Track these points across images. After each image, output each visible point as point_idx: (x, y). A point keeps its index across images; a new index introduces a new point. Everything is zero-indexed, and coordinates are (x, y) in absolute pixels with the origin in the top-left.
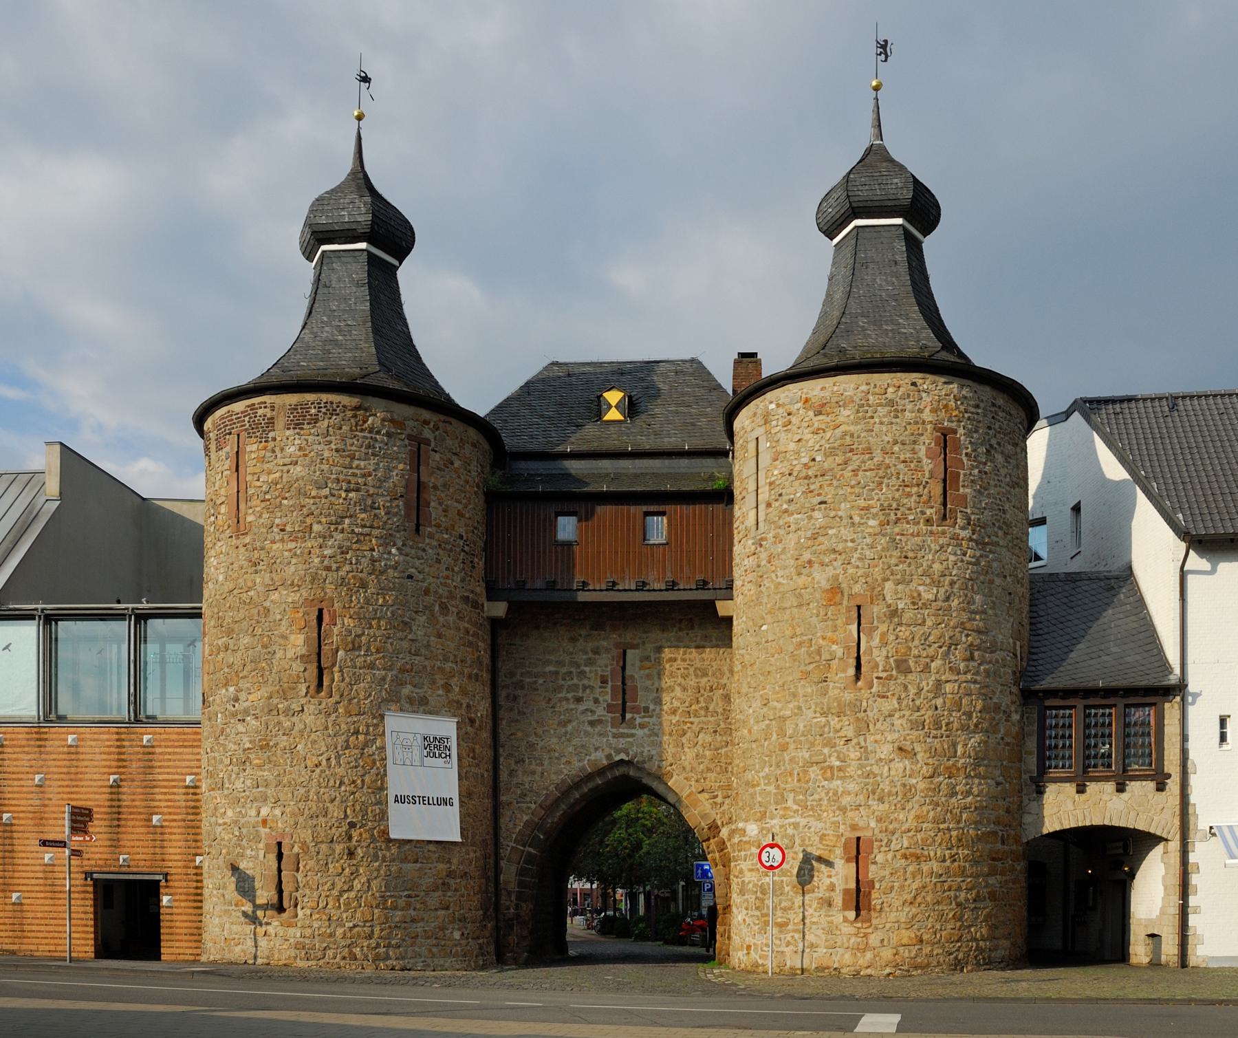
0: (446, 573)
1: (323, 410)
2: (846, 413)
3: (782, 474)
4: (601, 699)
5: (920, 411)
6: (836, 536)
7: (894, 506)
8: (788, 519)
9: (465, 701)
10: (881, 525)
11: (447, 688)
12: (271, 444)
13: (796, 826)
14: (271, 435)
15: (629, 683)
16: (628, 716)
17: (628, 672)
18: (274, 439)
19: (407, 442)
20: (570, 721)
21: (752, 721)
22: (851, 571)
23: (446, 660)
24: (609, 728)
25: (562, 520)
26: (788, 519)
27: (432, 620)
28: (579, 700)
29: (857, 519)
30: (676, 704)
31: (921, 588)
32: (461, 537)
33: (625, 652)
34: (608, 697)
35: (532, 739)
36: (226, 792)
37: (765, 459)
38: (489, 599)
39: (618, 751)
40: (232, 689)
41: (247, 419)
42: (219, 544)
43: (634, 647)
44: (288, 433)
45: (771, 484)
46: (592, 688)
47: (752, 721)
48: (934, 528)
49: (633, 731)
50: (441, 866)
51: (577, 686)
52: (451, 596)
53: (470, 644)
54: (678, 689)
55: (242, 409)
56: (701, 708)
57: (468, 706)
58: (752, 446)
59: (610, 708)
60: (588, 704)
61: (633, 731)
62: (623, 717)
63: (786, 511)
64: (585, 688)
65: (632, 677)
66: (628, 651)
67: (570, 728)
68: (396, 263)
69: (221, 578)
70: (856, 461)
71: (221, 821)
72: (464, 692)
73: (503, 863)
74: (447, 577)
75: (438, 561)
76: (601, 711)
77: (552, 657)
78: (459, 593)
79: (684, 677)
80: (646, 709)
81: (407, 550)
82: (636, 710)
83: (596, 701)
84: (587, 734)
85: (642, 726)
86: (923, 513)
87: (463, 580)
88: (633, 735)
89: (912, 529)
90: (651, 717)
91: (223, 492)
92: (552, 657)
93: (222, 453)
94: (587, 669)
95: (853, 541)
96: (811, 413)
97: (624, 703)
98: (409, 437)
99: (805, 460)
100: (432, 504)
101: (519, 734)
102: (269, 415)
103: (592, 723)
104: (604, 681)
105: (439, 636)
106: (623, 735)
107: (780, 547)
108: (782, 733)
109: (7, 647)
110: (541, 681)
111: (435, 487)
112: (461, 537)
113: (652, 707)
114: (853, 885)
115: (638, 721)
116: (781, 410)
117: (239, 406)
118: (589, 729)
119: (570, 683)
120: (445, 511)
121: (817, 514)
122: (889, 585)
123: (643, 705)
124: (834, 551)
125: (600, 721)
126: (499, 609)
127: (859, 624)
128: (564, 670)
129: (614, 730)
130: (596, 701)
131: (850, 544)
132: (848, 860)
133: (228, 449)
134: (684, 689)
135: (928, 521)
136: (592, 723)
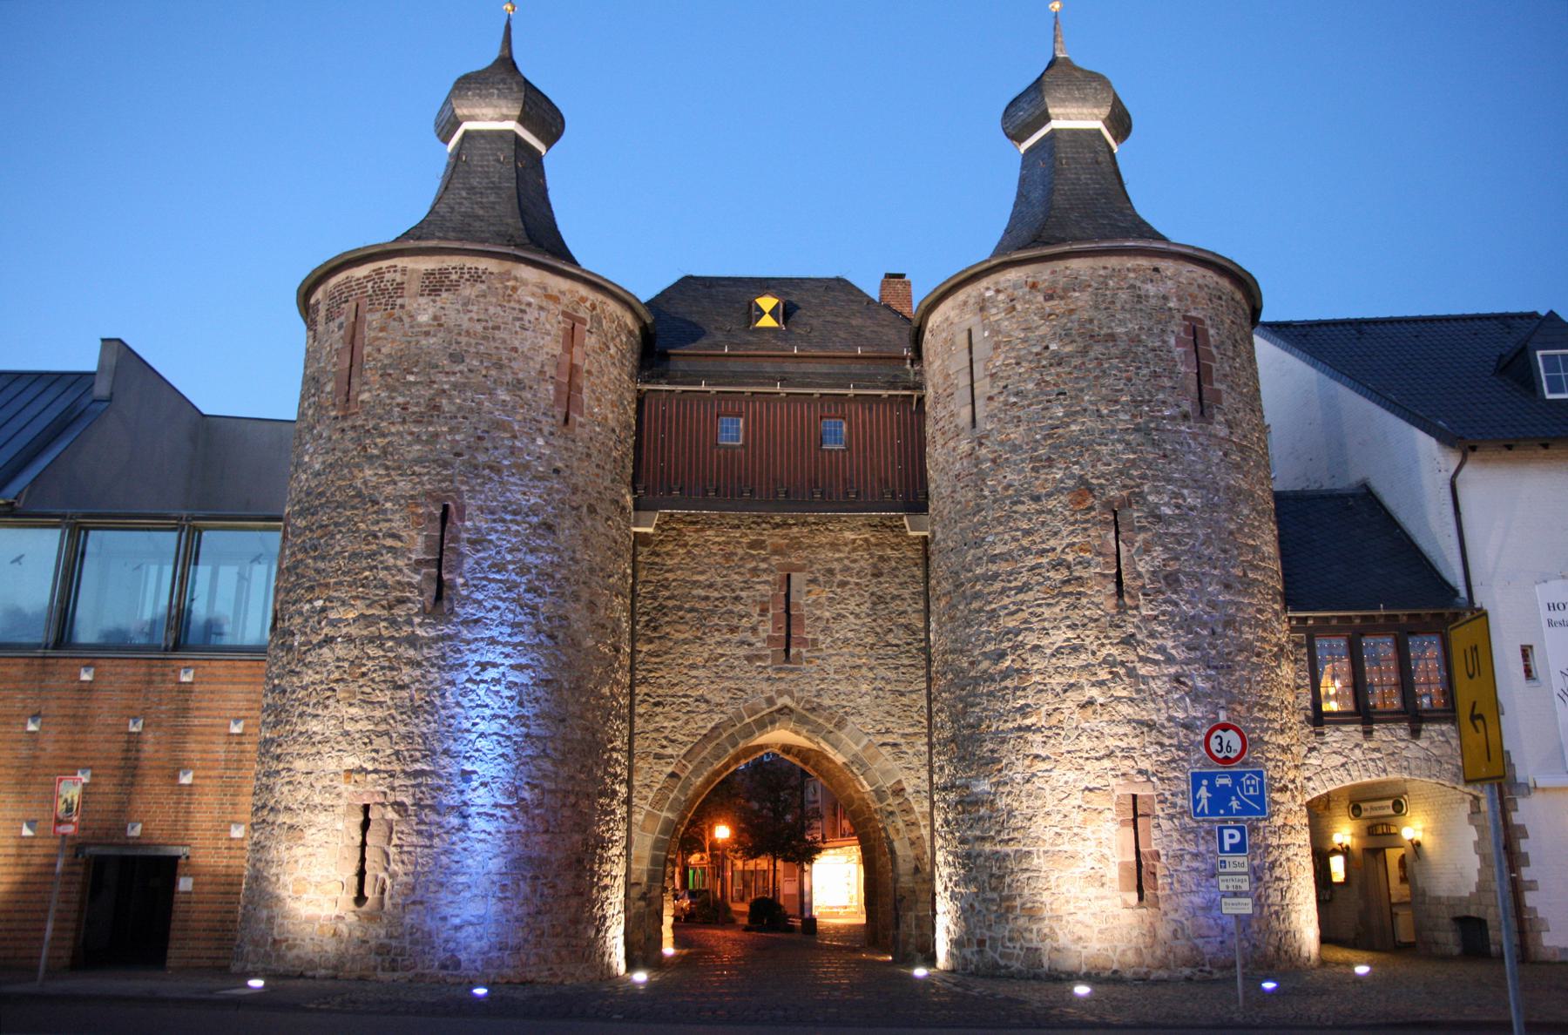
2: (1081, 298)
5: (1165, 298)
12: (397, 312)
14: (399, 301)
16: (793, 651)
18: (402, 306)
19: (560, 318)
25: (725, 422)
34: (769, 626)
43: (800, 569)
45: (992, 375)
58: (962, 339)
62: (787, 651)
65: (798, 604)
66: (794, 575)
68: (541, 147)
70: (1097, 350)
80: (815, 641)
93: (333, 325)
96: (1040, 298)
97: (788, 635)
98: (564, 313)
109: (18, 560)
114: (1133, 858)
116: (1001, 297)
127: (1117, 533)
132: (1123, 823)
135: (1185, 417)
136: (749, 659)
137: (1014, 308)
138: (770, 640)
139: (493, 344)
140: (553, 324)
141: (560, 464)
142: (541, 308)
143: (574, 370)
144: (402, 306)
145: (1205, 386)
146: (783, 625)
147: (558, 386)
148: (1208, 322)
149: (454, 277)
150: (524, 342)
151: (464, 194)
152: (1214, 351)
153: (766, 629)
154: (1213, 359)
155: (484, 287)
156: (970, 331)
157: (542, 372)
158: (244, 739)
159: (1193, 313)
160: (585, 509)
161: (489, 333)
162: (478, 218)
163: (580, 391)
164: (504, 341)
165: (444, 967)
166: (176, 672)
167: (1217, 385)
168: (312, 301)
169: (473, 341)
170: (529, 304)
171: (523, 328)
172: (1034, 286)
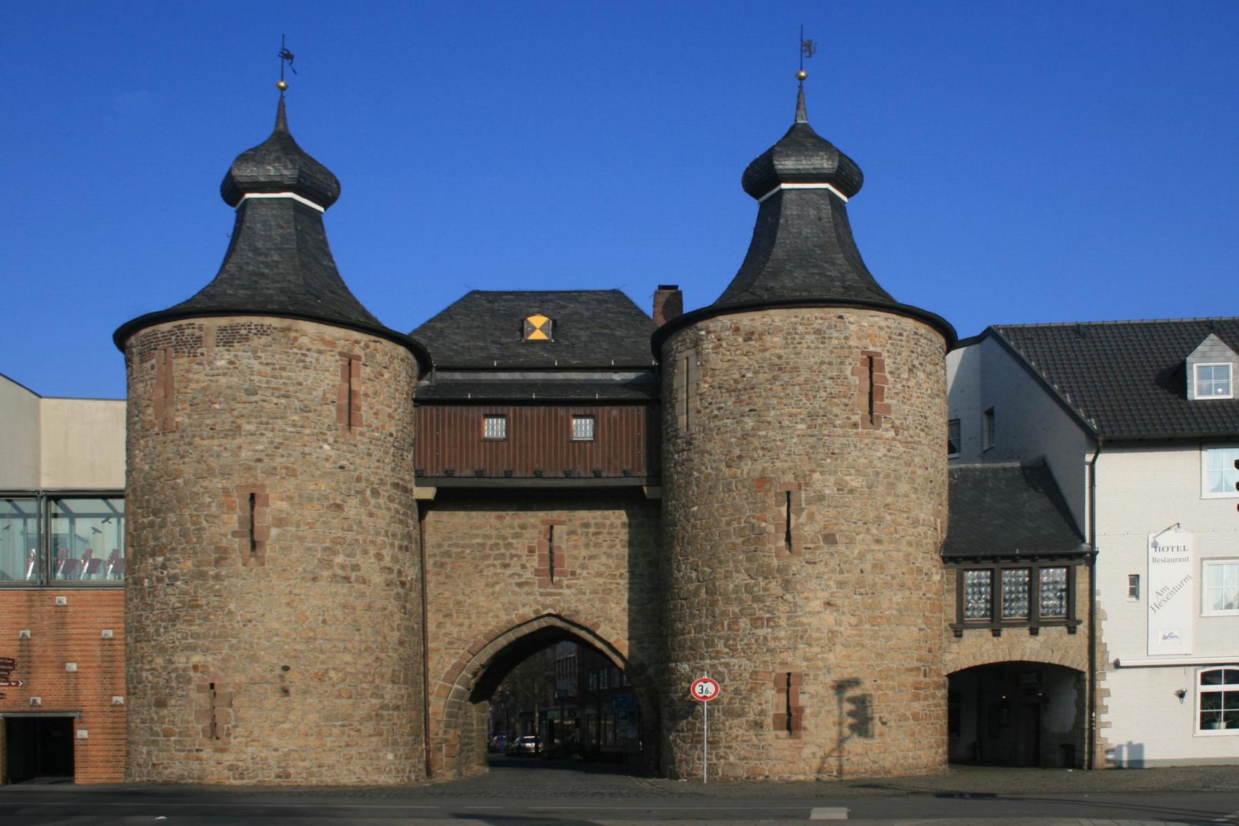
0: (377, 464)
8: (718, 423)
9: (396, 568)
11: (379, 557)
14: (199, 351)
16: (556, 579)
17: (556, 542)
20: (497, 583)
23: (378, 534)
26: (718, 423)
27: (364, 502)
32: (391, 435)
35: (460, 597)
38: (417, 485)
44: (216, 349)
46: (519, 556)
48: (860, 430)
50: (373, 701)
52: (382, 482)
53: (401, 522)
57: (400, 572)
63: (716, 416)
64: (512, 556)
67: (497, 588)
72: (395, 559)
73: (431, 698)
74: (378, 468)
75: (370, 455)
76: (528, 575)
77: (479, 532)
78: (389, 481)
79: (611, 547)
81: (336, 446)
84: (514, 593)
85: (569, 587)
87: (393, 470)
88: (560, 594)
92: (479, 532)
97: (552, 568)
98: (341, 354)
99: (737, 376)
100: (363, 408)
101: (447, 594)
103: (519, 585)
105: (371, 515)
110: (468, 551)
111: (366, 395)
112: (391, 435)
113: (579, 571)
115: (565, 582)
118: (517, 589)
120: (376, 414)
125: (526, 583)
126: (428, 493)
136: (519, 585)
138: (537, 572)
140: (332, 362)
141: (344, 463)
142: (320, 352)
143: (351, 394)
145: (876, 403)
147: (339, 410)
149: (243, 332)
150: (308, 377)
153: (535, 563)
154: (885, 380)
155: (270, 338)
157: (324, 398)
160: (368, 492)
161: (277, 373)
163: (359, 409)
164: (290, 378)
165: (278, 776)
166: (52, 598)
169: (264, 379)
170: (309, 350)
171: (305, 368)
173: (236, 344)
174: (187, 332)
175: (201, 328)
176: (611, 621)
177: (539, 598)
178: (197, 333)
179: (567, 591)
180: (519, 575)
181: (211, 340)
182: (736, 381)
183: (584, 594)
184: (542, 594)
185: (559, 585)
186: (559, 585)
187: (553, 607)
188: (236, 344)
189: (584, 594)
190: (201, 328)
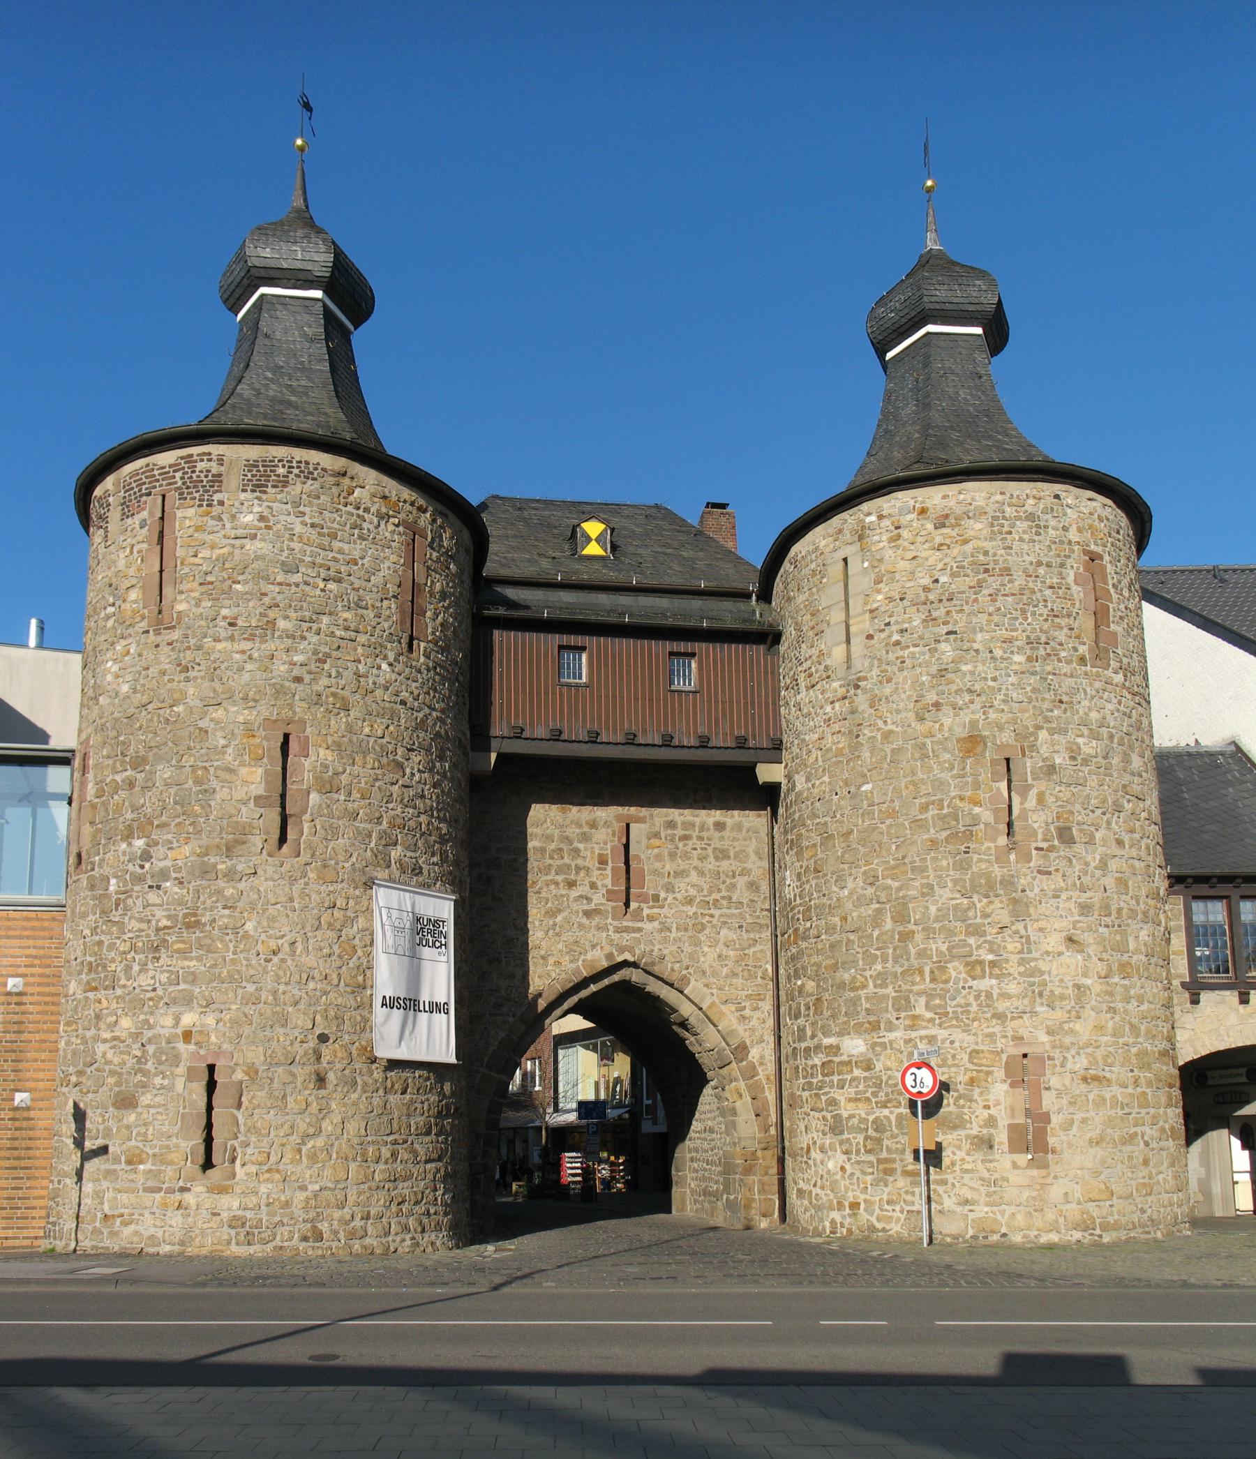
1: (296, 471)
2: (977, 527)
3: (891, 599)
4: (599, 884)
5: (1065, 529)
6: (972, 673)
7: (1043, 639)
10: (1029, 659)
12: (216, 510)
13: (931, 1039)
14: (216, 497)
15: (633, 865)
16: (633, 905)
18: (221, 503)
20: (559, 911)
21: (849, 906)
22: (993, 715)
24: (610, 920)
28: (571, 884)
29: (998, 653)
30: (692, 892)
31: (1080, 740)
33: (628, 826)
34: (608, 882)
36: (119, 992)
37: (859, 583)
39: (622, 950)
40: (139, 843)
41: (179, 475)
42: (123, 642)
44: (243, 496)
47: (849, 906)
49: (639, 925)
51: (569, 866)
54: (693, 873)
55: (172, 461)
56: (723, 898)
59: (610, 895)
60: (583, 889)
61: (639, 925)
62: (627, 905)
63: (897, 643)
65: (637, 857)
67: (559, 918)
68: (351, 327)
69: (125, 688)
70: (993, 583)
71: (107, 1035)
76: (598, 899)
80: (656, 898)
82: (643, 898)
83: (593, 886)
84: (581, 926)
85: (651, 919)
86: (1075, 649)
88: (639, 930)
89: (1066, 668)
90: (662, 907)
91: (132, 572)
94: (581, 846)
95: (994, 679)
96: (930, 526)
99: (926, 581)
102: (214, 471)
103: (587, 914)
104: (603, 861)
106: (627, 930)
107: (888, 690)
108: (901, 917)
115: (646, 912)
116: (886, 523)
117: (166, 458)
118: (584, 920)
119: (560, 862)
121: (943, 646)
122: (1043, 735)
123: (651, 892)
124: (970, 691)
125: (597, 911)
127: (1009, 782)
128: (553, 846)
129: (616, 923)
130: (593, 886)
131: (991, 683)
133: (145, 514)
134: (702, 874)
135: (1082, 660)
136: (587, 914)
137: (899, 537)
139: (331, 555)
144: (221, 503)
146: (623, 880)
148: (1107, 558)
149: (281, 471)
151: (269, 375)
152: (1112, 591)
155: (317, 485)
156: (845, 560)
158: (24, 999)
159: (1093, 547)
162: (290, 404)
167: (1113, 627)
168: (98, 492)
172: (923, 511)
173: (269, 490)
174: (200, 466)
175: (221, 462)
176: (704, 973)
177: (615, 936)
178: (215, 469)
179: (648, 926)
180: (589, 900)
181: (233, 480)
182: (926, 589)
183: (669, 930)
184: (618, 930)
185: (638, 916)
186: (638, 916)
187: (631, 950)
188: (269, 490)
189: (669, 930)
190: (221, 462)
